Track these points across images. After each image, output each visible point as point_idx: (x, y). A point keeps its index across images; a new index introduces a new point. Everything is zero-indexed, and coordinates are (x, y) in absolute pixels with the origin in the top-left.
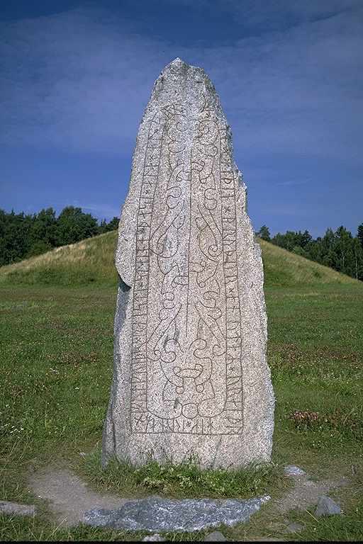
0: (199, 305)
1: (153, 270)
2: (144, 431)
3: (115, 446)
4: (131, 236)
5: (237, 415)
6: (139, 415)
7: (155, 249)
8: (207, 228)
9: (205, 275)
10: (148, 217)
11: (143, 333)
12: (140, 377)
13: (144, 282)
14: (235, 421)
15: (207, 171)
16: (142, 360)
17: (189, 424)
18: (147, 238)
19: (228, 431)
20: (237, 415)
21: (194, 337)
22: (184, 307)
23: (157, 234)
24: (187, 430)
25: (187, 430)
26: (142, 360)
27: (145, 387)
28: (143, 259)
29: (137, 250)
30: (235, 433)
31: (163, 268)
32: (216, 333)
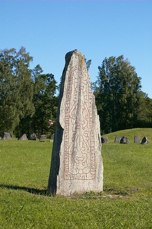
0: (83, 136)
1: (70, 124)
4: (64, 111)
5: (93, 173)
6: (67, 173)
7: (70, 116)
9: (84, 126)
11: (67, 145)
12: (66, 160)
13: (68, 128)
14: (93, 175)
15: (84, 90)
16: (67, 154)
17: (80, 176)
19: (91, 178)
20: (93, 173)
21: (82, 146)
22: (79, 136)
23: (71, 111)
24: (80, 178)
25: (80, 178)
26: (67, 154)
27: (68, 164)
30: (93, 179)
31: (73, 123)
32: (88, 145)
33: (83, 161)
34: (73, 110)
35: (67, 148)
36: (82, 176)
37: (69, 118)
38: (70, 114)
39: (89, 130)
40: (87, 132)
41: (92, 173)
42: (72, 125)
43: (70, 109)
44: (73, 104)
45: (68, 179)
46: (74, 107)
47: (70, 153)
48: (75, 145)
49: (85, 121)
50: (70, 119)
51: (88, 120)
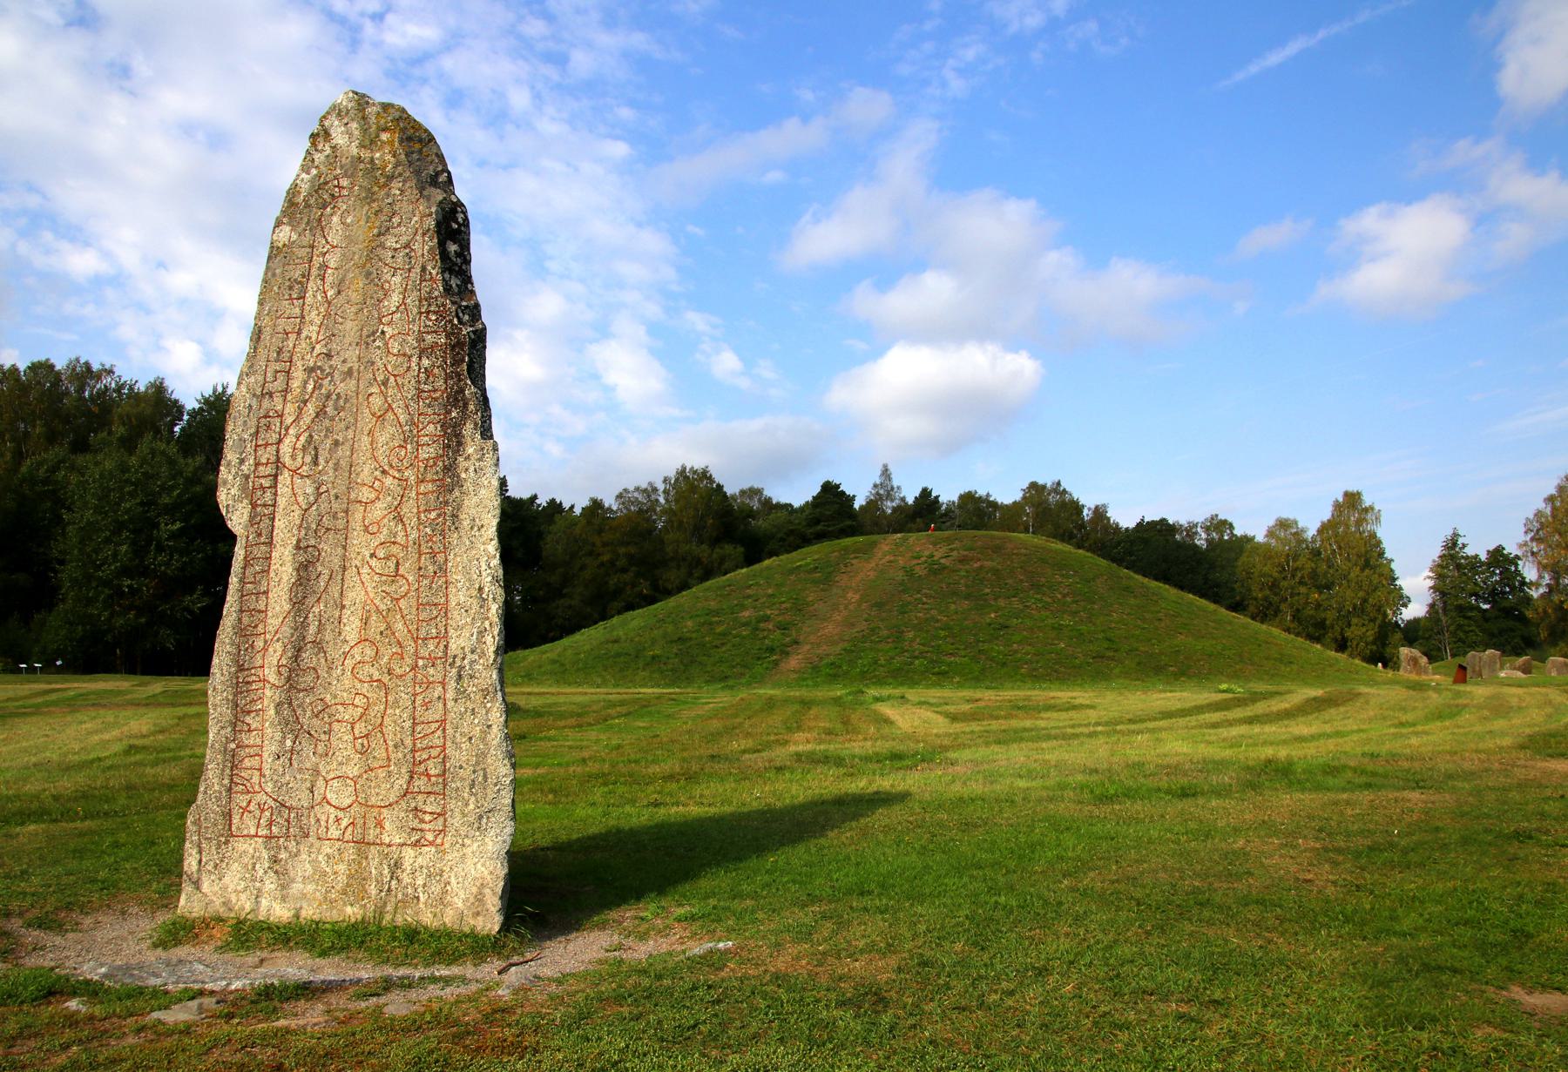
0: (365, 570)
1: (282, 502)
2: (253, 832)
3: (200, 861)
7: (287, 460)
8: (390, 414)
9: (378, 510)
10: (278, 399)
11: (260, 629)
17: (338, 820)
18: (275, 437)
28: (266, 483)
29: (257, 464)
31: (300, 499)
32: (400, 626)
33: (360, 728)
34: (307, 419)
35: (259, 644)
36: (344, 823)
37: (276, 476)
38: (286, 448)
39: (414, 535)
40: (395, 549)
41: (421, 805)
42: (298, 512)
43: (289, 420)
44: (310, 387)
45: (256, 836)
46: (311, 409)
47: (273, 678)
48: (312, 629)
49: (388, 481)
50: (285, 477)
51: (410, 474)
